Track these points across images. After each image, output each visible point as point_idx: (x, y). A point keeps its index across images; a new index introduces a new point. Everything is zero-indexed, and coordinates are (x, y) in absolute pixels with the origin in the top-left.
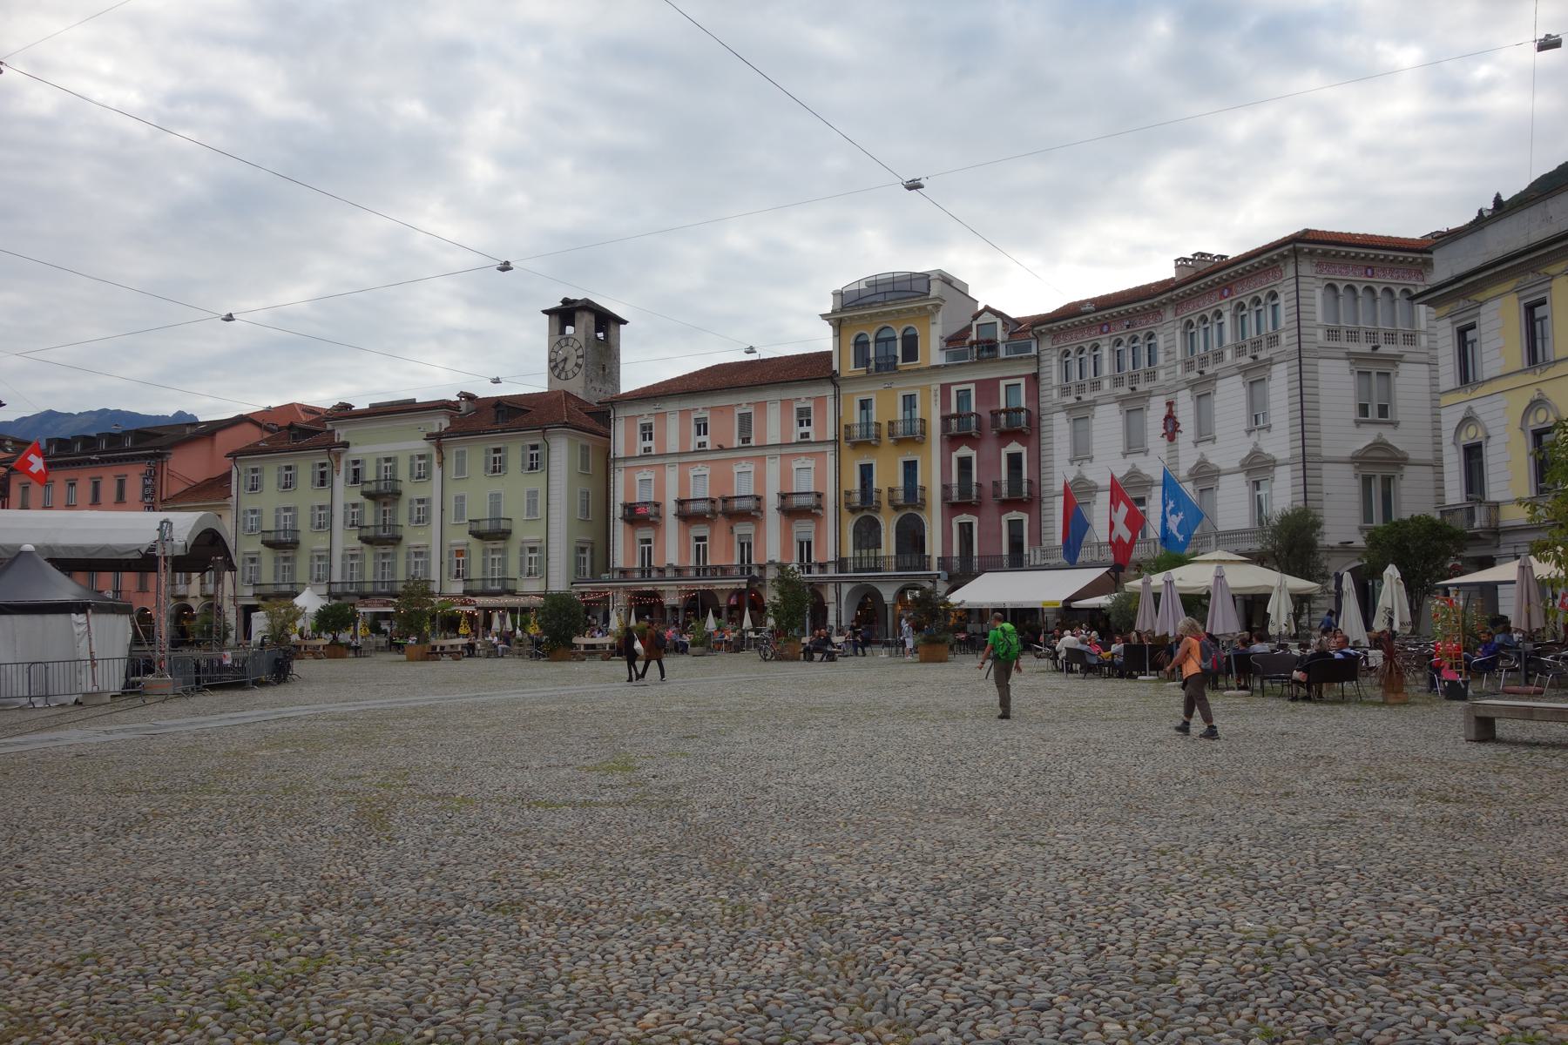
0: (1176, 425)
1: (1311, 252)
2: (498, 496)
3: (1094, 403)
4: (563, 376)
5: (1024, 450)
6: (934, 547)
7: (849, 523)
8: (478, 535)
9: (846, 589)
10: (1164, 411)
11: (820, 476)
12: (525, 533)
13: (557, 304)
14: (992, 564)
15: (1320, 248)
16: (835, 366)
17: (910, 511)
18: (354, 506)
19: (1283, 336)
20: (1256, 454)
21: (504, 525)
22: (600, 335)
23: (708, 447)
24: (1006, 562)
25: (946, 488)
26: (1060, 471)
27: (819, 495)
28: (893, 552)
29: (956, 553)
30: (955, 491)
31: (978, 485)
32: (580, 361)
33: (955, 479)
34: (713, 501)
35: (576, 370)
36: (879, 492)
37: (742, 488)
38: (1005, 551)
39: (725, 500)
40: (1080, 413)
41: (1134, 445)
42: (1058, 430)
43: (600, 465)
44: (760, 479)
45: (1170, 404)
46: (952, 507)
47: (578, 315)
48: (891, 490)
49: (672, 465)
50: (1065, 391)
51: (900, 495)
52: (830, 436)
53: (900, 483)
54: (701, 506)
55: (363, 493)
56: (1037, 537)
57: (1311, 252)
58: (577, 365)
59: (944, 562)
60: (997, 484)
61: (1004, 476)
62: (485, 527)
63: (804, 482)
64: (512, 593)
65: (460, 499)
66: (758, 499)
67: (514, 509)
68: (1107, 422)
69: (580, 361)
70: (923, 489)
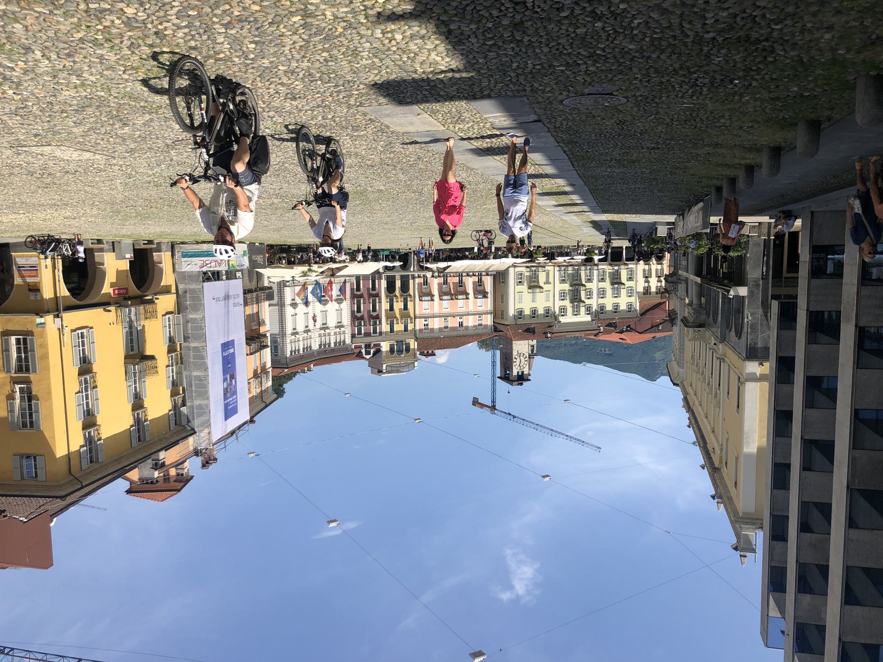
0: (313, 319)
1: (283, 365)
2: (533, 301)
3: (336, 327)
4: (522, 354)
5: (356, 314)
6: (384, 283)
7: (411, 292)
8: (541, 288)
9: (412, 269)
10: (316, 323)
11: (421, 307)
12: (524, 288)
13: (525, 383)
14: (366, 277)
15: (280, 366)
16: (416, 343)
17: (391, 295)
18: (589, 298)
19: (289, 342)
20: (295, 308)
21: (530, 291)
22: (508, 372)
23: (458, 317)
24: (361, 278)
25: (380, 302)
26: (346, 306)
27: (421, 300)
28: (397, 281)
29: (377, 281)
30: (377, 301)
31: (370, 303)
32: (515, 360)
33: (377, 304)
34: (457, 299)
35: (516, 357)
36: (401, 301)
37: (445, 304)
38: (361, 281)
39: (452, 299)
40: (340, 326)
41: (325, 312)
42: (346, 320)
43: (498, 311)
44: (441, 306)
45: (315, 326)
46: (378, 295)
47: (516, 379)
48: (397, 302)
49: (471, 311)
50: (344, 333)
51: (395, 300)
52: (417, 320)
53: (395, 304)
54: (460, 297)
55: (585, 302)
56: (352, 284)
57: (283, 365)
58: (516, 359)
59: (380, 278)
60: (364, 303)
61: (362, 305)
62: (538, 290)
63: (426, 305)
64: (527, 267)
65: (548, 300)
66: (441, 300)
67: (527, 295)
68: (332, 322)
69: (515, 360)
70: (387, 302)
